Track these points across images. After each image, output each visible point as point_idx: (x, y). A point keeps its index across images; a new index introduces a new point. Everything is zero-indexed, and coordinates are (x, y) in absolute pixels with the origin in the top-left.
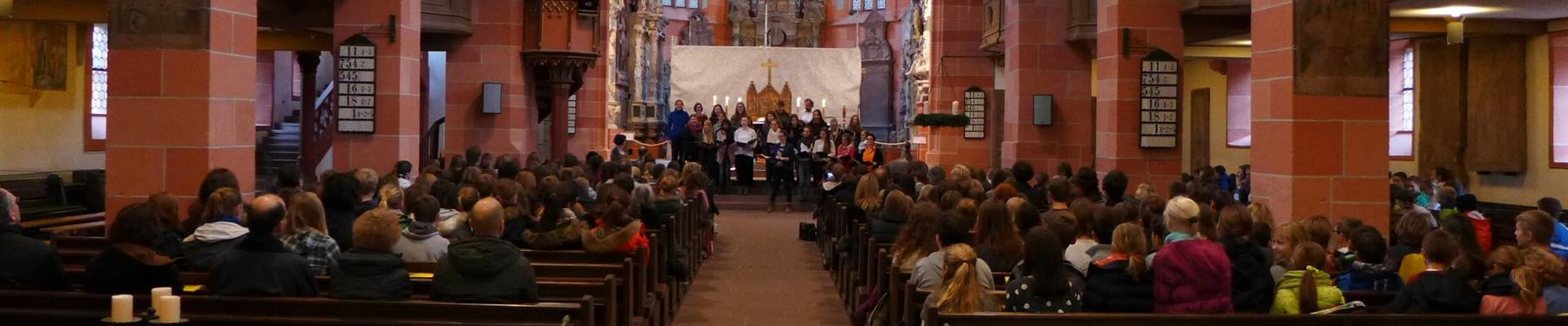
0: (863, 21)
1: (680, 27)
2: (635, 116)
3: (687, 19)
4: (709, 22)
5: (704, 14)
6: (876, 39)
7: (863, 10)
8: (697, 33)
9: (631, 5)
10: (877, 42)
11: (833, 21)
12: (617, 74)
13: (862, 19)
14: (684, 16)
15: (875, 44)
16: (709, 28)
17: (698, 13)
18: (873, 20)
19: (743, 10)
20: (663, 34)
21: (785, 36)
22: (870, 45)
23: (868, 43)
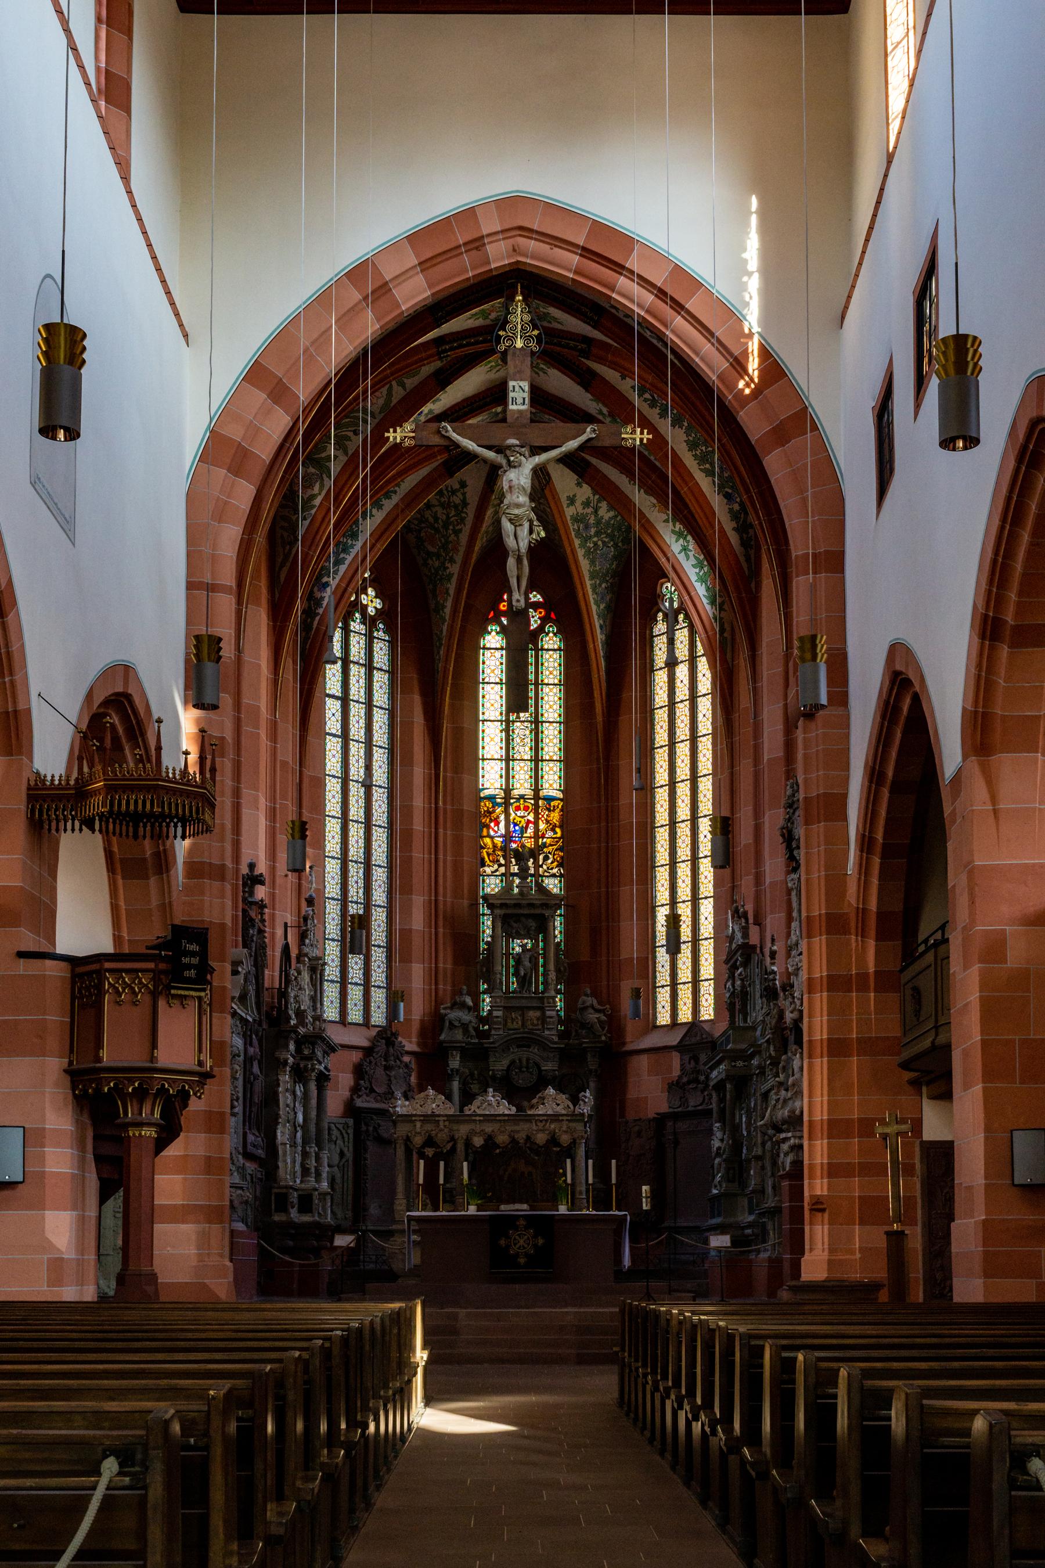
0: (675, 1043)
1: (356, 1056)
2: (276, 1211)
3: (365, 1043)
4: (406, 1048)
5: (395, 1035)
6: (698, 1072)
7: (674, 1024)
8: (387, 1068)
9: (268, 1015)
10: (702, 1078)
11: (624, 1044)
12: (245, 1135)
13: (674, 1039)
14: (360, 1039)
15: (697, 1081)
16: (406, 1059)
17: (387, 1036)
18: (694, 1040)
19: (465, 1026)
20: (326, 1068)
21: (540, 1071)
22: (689, 1082)
23: (685, 1080)
